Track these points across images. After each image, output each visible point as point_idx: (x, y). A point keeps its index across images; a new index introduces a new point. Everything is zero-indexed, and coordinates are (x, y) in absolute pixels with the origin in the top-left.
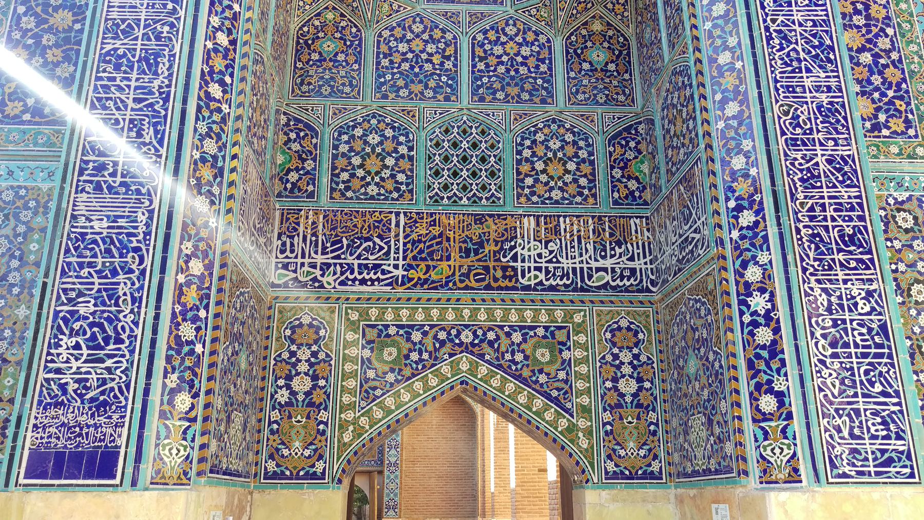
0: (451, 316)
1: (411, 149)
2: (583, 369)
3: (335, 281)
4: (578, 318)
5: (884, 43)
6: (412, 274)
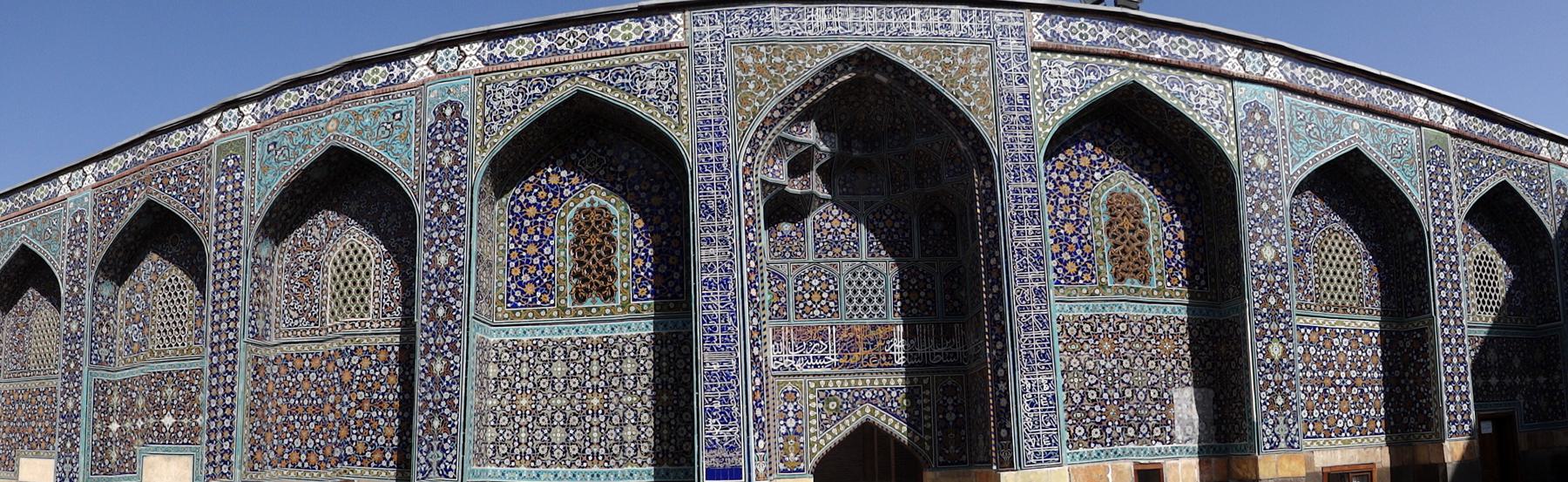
0: (860, 383)
1: (836, 287)
2: (928, 409)
4: (925, 382)
5: (1084, 230)
6: (841, 360)
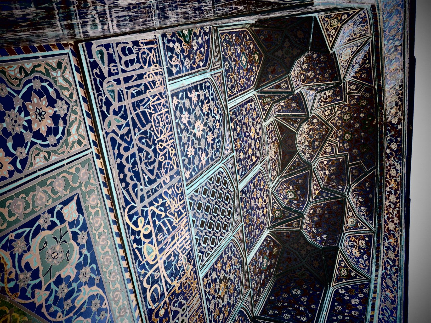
3: (114, 132)
